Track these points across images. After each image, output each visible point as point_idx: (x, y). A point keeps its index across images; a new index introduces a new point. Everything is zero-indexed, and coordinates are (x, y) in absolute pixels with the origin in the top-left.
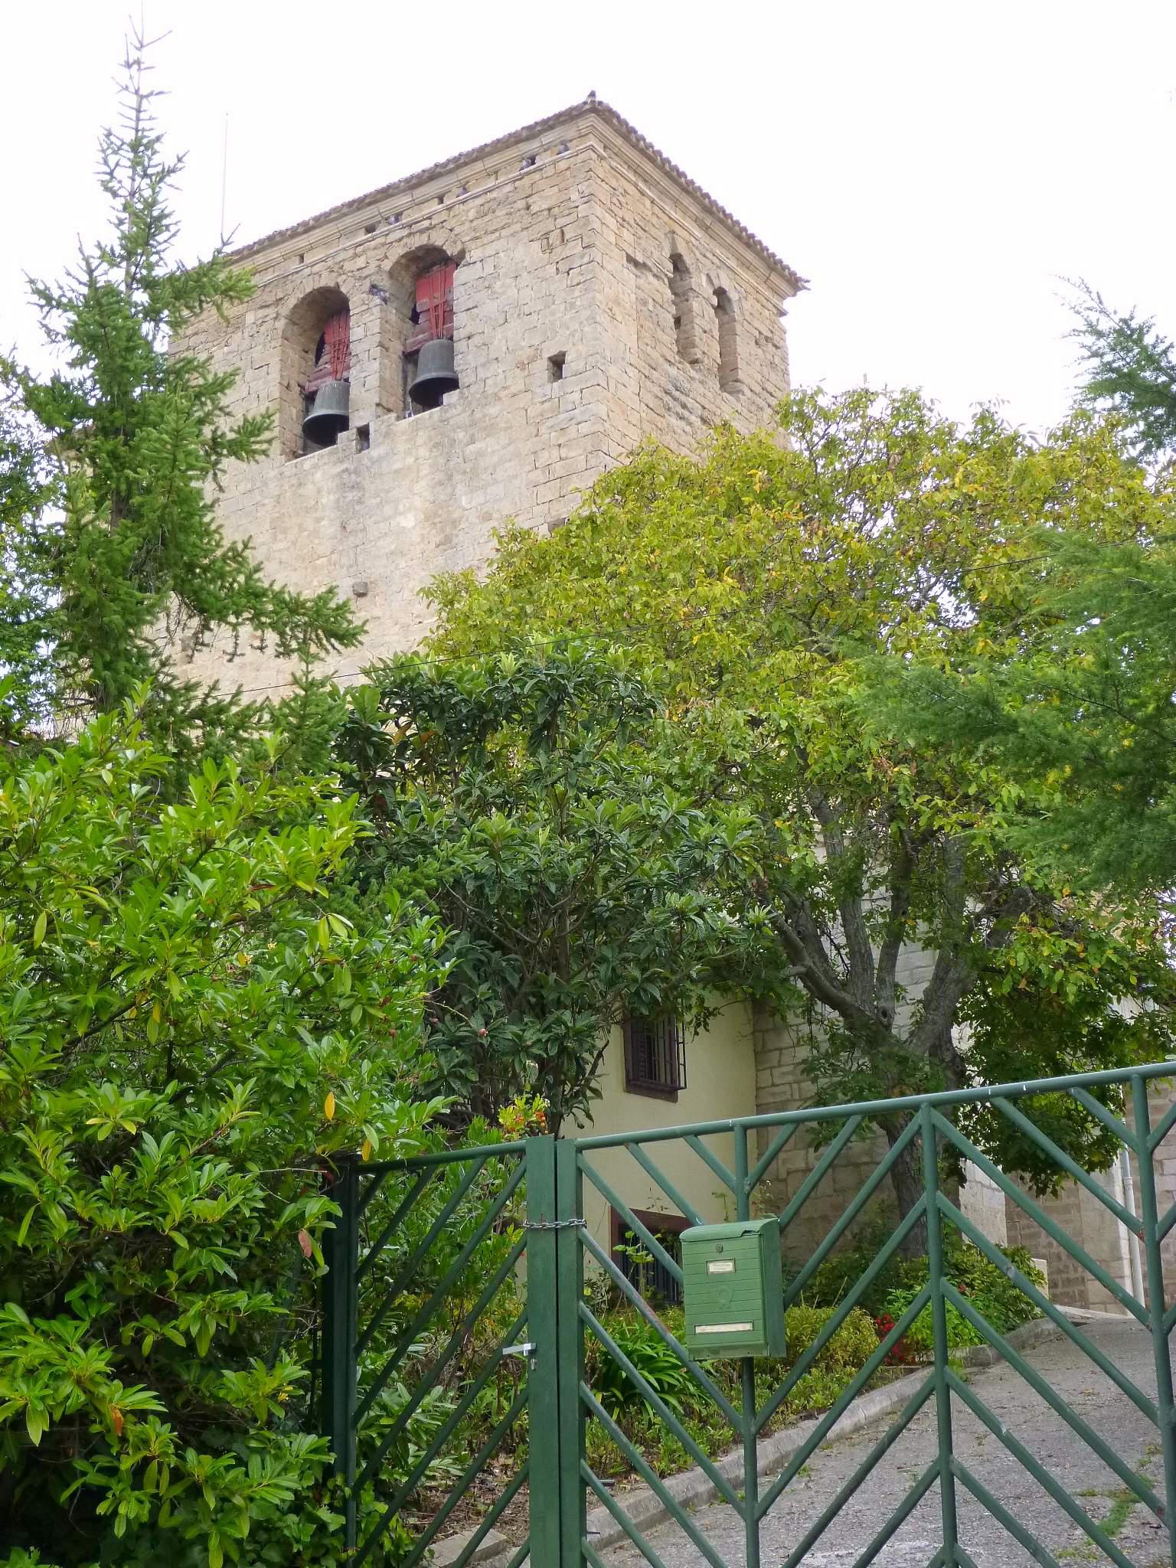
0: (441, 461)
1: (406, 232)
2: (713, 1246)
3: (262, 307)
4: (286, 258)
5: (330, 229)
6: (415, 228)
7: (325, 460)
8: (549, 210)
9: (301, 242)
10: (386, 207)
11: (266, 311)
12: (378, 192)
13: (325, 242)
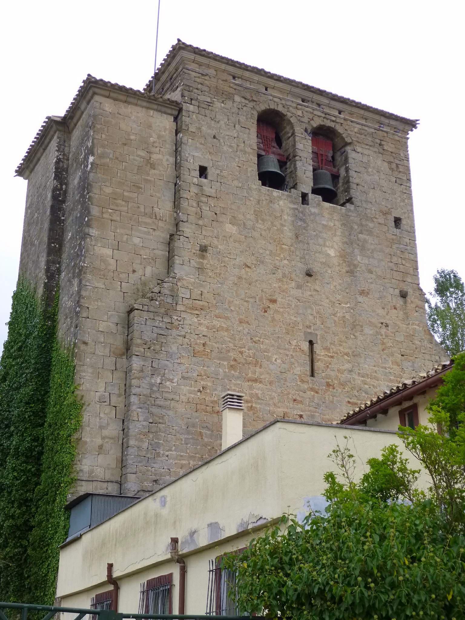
0: (347, 233)
1: (323, 115)
2: (305, 420)
3: (243, 97)
4: (259, 83)
5: (288, 87)
6: (327, 116)
7: (285, 197)
8: (392, 153)
9: (271, 82)
10: (316, 97)
11: (243, 100)
12: (319, 90)
13: (280, 90)
